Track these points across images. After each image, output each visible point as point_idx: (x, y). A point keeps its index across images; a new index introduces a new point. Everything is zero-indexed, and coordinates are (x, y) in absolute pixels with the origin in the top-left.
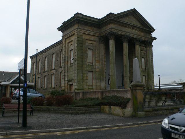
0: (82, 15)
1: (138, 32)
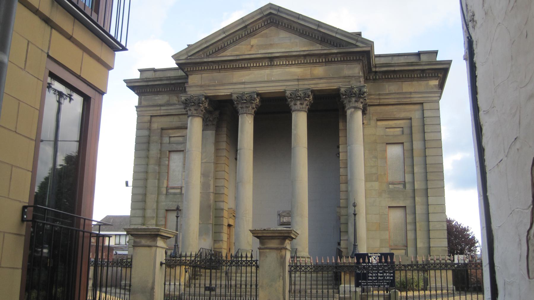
0: (152, 72)
1: (297, 71)
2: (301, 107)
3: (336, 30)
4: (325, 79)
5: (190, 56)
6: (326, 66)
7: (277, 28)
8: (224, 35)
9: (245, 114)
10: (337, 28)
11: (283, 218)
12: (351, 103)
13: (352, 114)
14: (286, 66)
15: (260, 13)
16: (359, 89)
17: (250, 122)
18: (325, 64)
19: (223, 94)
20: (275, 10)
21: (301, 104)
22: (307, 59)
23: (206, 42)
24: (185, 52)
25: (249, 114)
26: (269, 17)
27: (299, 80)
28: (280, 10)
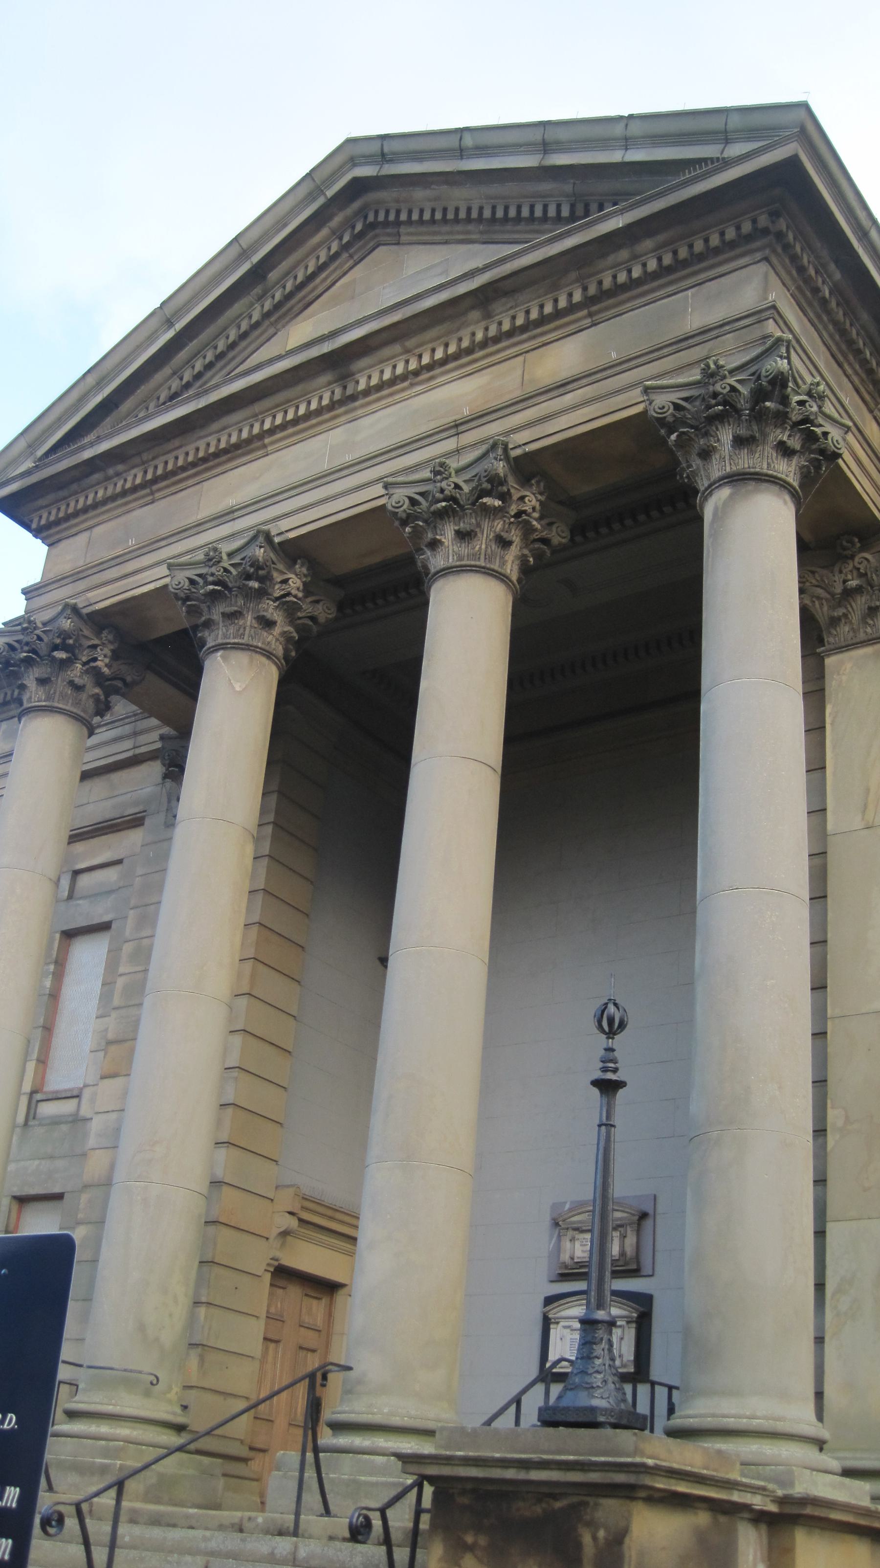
2: (464, 550)
3: (618, 130)
4: (584, 381)
5: (40, 459)
6: (594, 325)
7: (398, 244)
8: (170, 334)
9: (217, 650)
10: (621, 118)
11: (573, 1240)
12: (715, 458)
13: (720, 515)
14: (412, 385)
15: (311, 197)
16: (753, 374)
17: (238, 689)
18: (590, 315)
19: (151, 587)
20: (368, 159)
21: (463, 536)
22: (497, 318)
23: (99, 385)
24: (22, 444)
25: (237, 647)
26: (356, 205)
27: (461, 428)
28: (386, 150)
